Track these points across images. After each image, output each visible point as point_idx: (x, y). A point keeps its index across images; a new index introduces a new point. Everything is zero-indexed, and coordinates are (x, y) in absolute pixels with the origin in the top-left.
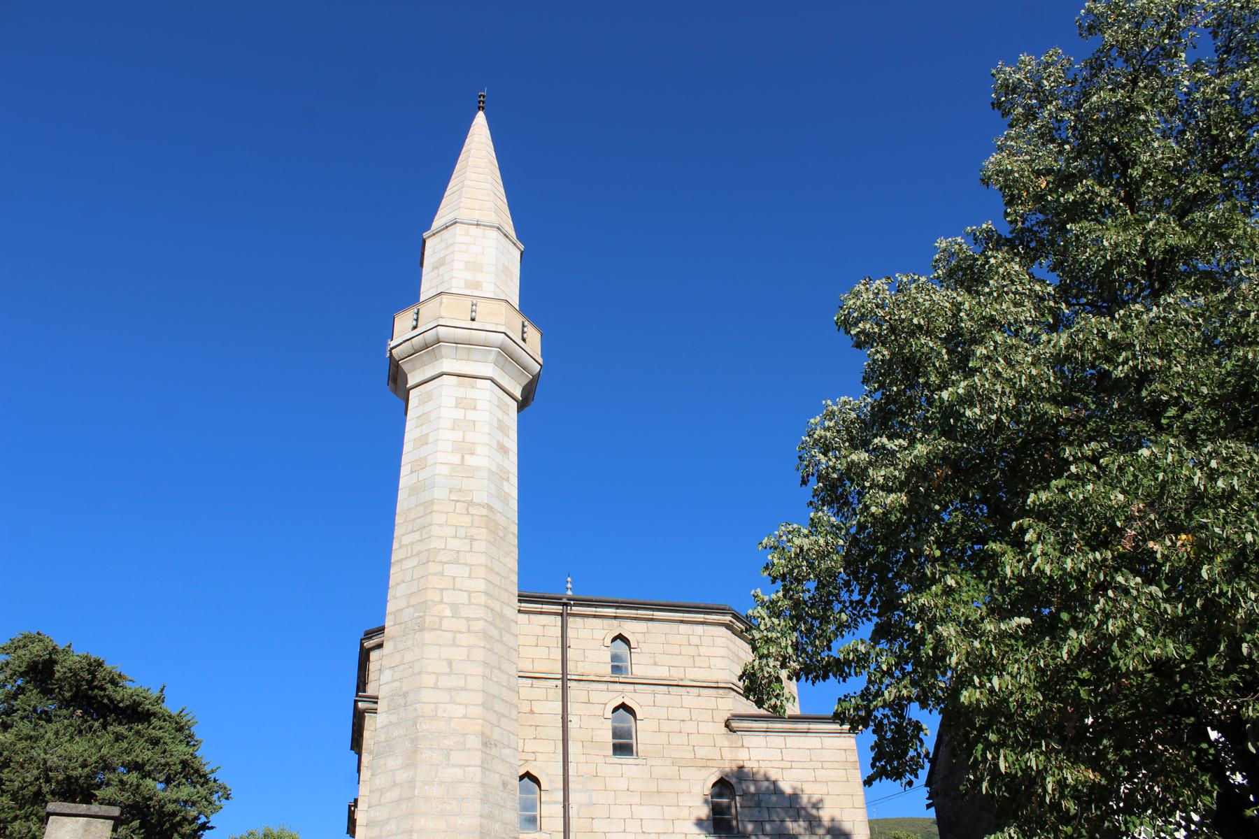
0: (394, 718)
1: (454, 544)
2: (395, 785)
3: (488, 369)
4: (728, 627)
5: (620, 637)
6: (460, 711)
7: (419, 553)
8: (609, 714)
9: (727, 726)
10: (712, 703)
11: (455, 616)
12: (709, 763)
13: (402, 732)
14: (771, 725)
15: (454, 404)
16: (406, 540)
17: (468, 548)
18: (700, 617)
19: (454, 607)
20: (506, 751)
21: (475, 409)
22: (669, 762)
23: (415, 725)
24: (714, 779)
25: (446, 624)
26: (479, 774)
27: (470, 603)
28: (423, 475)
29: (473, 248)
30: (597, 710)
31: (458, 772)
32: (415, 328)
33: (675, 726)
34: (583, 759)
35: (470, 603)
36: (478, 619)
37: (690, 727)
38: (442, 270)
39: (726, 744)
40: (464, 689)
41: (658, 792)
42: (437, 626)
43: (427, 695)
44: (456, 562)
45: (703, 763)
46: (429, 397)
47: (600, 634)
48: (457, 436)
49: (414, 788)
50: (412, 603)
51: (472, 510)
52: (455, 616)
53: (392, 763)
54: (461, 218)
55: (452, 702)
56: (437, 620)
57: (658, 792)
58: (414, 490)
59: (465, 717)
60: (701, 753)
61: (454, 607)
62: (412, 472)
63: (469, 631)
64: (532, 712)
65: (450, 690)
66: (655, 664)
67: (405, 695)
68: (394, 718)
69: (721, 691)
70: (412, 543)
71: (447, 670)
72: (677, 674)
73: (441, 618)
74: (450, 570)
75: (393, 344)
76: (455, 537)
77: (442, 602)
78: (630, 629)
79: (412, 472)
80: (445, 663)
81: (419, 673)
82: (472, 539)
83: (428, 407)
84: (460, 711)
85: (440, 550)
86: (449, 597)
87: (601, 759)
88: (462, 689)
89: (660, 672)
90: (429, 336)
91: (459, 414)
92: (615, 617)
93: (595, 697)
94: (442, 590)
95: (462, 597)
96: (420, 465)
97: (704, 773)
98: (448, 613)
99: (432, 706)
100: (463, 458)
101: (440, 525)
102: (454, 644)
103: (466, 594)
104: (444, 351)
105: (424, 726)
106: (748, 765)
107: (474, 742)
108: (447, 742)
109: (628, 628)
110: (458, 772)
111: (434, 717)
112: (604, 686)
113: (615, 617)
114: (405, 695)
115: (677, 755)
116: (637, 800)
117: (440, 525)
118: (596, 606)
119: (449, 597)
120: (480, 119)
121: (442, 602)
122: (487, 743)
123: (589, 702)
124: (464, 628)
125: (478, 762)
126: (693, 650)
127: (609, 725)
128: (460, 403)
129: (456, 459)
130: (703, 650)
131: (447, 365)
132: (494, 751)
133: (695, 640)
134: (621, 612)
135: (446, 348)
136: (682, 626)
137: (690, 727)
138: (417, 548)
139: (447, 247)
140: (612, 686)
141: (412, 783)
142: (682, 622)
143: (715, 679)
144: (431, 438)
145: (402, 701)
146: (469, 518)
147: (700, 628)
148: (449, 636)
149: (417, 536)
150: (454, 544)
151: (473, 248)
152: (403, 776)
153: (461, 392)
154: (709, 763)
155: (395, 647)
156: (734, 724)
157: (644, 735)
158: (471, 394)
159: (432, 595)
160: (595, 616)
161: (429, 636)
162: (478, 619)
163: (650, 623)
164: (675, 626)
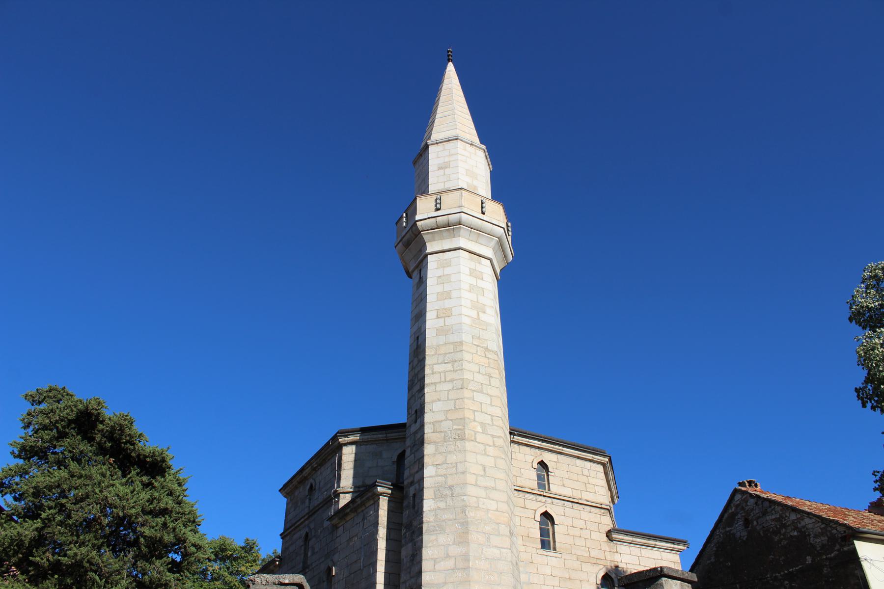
0: (442, 505)
1: (480, 378)
2: (448, 556)
3: (489, 253)
4: (604, 465)
5: (542, 464)
7: (452, 381)
9: (607, 536)
10: (598, 518)
12: (599, 562)
14: (634, 539)
16: (437, 368)
18: (590, 456)
19: (483, 424)
22: (575, 558)
23: (464, 512)
24: (602, 574)
25: (480, 437)
27: (493, 425)
28: (449, 321)
29: (459, 161)
31: (497, 551)
33: (577, 532)
34: (522, 548)
36: (499, 437)
37: (586, 534)
38: (447, 171)
39: (607, 549)
40: (494, 489)
41: (570, 579)
43: (471, 490)
44: (481, 392)
45: (594, 561)
46: (448, 264)
47: (529, 459)
49: (469, 560)
51: (489, 355)
53: (442, 539)
54: (461, 135)
55: (488, 498)
57: (570, 579)
58: (440, 331)
60: (594, 553)
61: (483, 424)
62: (438, 317)
63: (494, 445)
65: (486, 488)
66: (564, 485)
67: (451, 488)
68: (442, 505)
69: (603, 511)
71: (482, 473)
72: (577, 495)
73: (476, 433)
74: (479, 397)
75: (417, 218)
76: (479, 372)
77: (475, 420)
78: (548, 458)
79: (438, 317)
80: (481, 467)
81: (464, 473)
82: (490, 377)
83: (448, 271)
84: (493, 505)
86: (480, 417)
87: (534, 551)
88: (493, 488)
89: (566, 492)
90: (453, 218)
91: (473, 281)
92: (539, 448)
93: (529, 504)
94: (474, 411)
95: (487, 419)
96: (445, 314)
97: (596, 569)
98: (479, 429)
103: (489, 417)
104: (462, 231)
105: (471, 514)
106: (621, 565)
107: (504, 530)
108: (487, 528)
109: (548, 458)
111: (477, 508)
112: (533, 497)
113: (539, 448)
115: (579, 553)
116: (556, 583)
118: (529, 438)
119: (480, 417)
120: (451, 67)
121: (475, 420)
124: (491, 443)
126: (584, 479)
127: (537, 526)
128: (473, 273)
130: (591, 480)
131: (462, 242)
133: (586, 472)
134: (544, 445)
135: (464, 230)
136: (578, 461)
137: (586, 534)
138: (449, 377)
139: (450, 155)
140: (538, 497)
141: (466, 558)
142: (578, 458)
143: (599, 501)
144: (454, 294)
145: (448, 492)
147: (588, 464)
148: (482, 446)
149: (449, 367)
150: (480, 378)
151: (459, 161)
152: (456, 551)
153: (473, 265)
154: (599, 562)
156: (614, 536)
158: (479, 268)
159: (468, 414)
160: (526, 445)
161: (469, 445)
162: (499, 437)
163: (559, 456)
164: (574, 460)
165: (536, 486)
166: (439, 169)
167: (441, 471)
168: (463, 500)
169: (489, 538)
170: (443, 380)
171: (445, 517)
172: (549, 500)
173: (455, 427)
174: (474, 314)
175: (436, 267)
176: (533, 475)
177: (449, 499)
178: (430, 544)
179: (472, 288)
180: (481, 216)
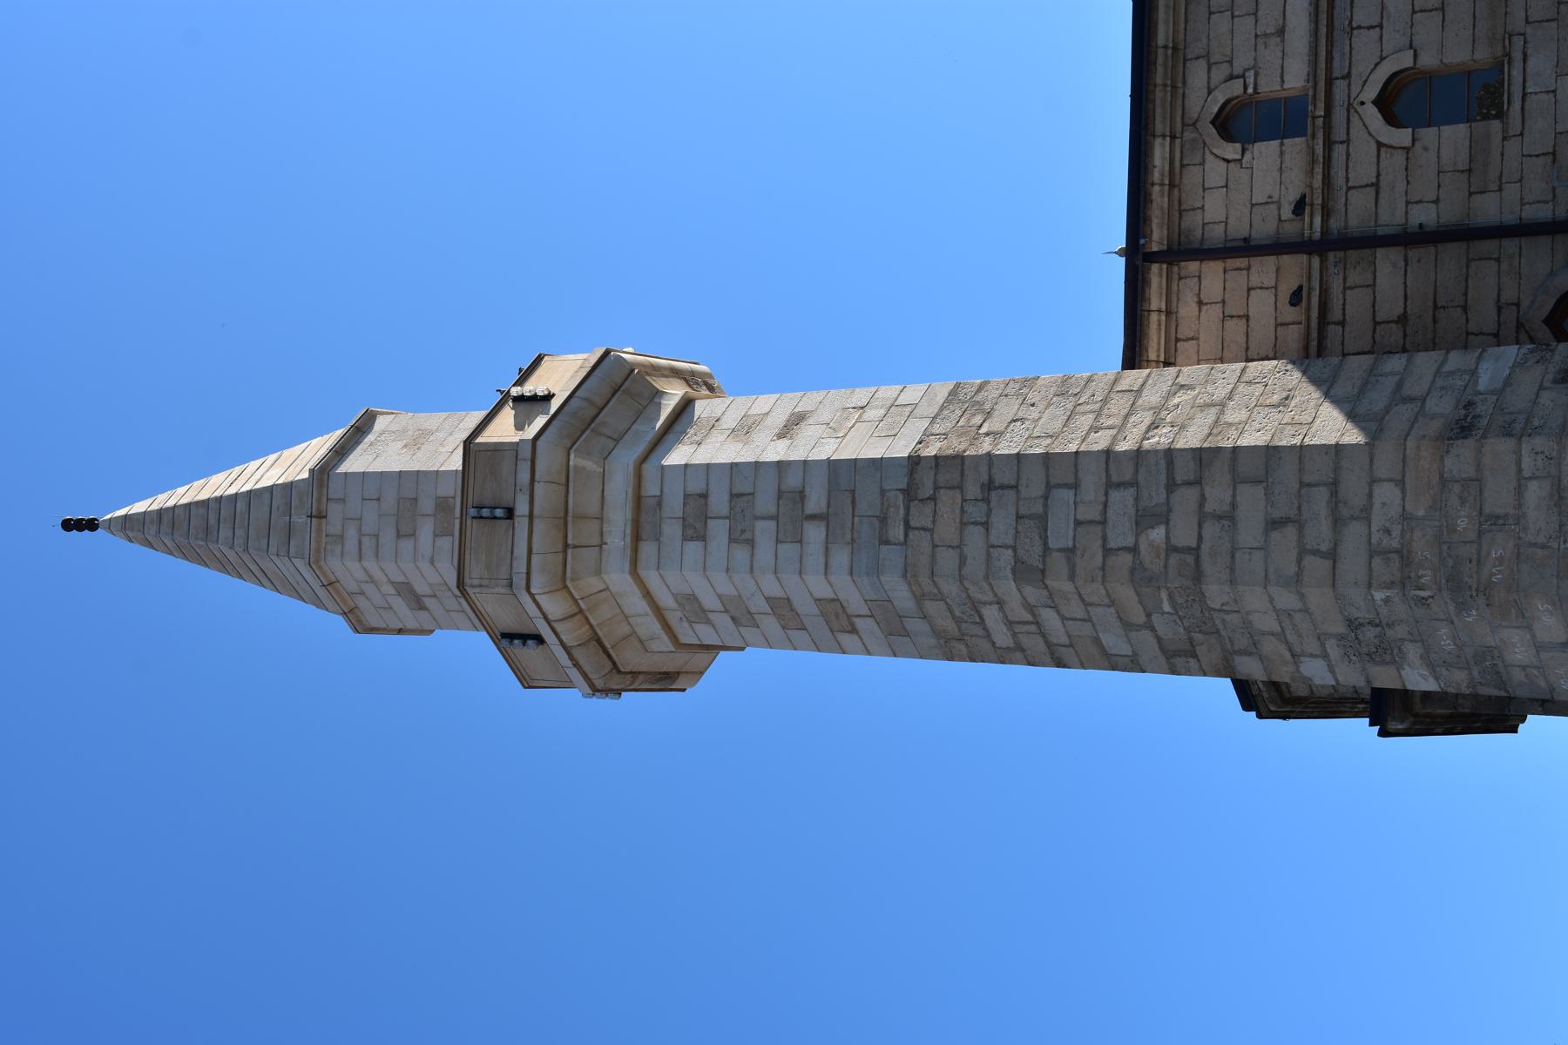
0: (1413, 652)
6: (1386, 493)
7: (1030, 608)
8: (1403, 136)
11: (1163, 517)
13: (1444, 631)
15: (700, 544)
17: (1011, 494)
19: (1144, 519)
20: (1484, 383)
21: (704, 496)
25: (1184, 535)
26: (1539, 442)
30: (1393, 164)
32: (539, 640)
34: (1512, 191)
35: (1134, 483)
38: (421, 588)
42: (1190, 559)
44: (1042, 520)
48: (764, 531)
50: (1142, 619)
51: (926, 491)
52: (1163, 517)
55: (1365, 514)
56: (1174, 559)
59: (1401, 483)
61: (1144, 519)
63: (1198, 482)
64: (1403, 319)
65: (1337, 522)
66: (1281, 32)
67: (1353, 625)
70: (1010, 624)
71: (1291, 531)
73: (1171, 549)
76: (986, 525)
77: (1134, 550)
80: (1275, 535)
84: (1386, 493)
85: (1017, 560)
86: (1121, 535)
87: (1513, 147)
88: (1334, 493)
93: (1363, 171)
94: (1107, 552)
98: (1157, 534)
99: (1377, 561)
100: (812, 517)
101: (963, 560)
102: (1229, 517)
103: (1115, 495)
107: (1461, 458)
108: (1462, 524)
110: (1535, 492)
112: (1339, 151)
114: (1353, 625)
117: (963, 560)
122: (1463, 428)
123: (1376, 186)
124: (1191, 494)
125: (1510, 443)
129: (815, 534)
132: (1484, 408)
140: (1339, 134)
145: (1370, 633)
146: (944, 496)
148: (1210, 529)
149: (991, 614)
153: (672, 530)
155: (1244, 652)
157: (1451, 47)
165: (1296, 145)
166: (423, 608)
167: (1312, 646)
168: (1387, 601)
169: (1497, 520)
170: (1033, 628)
171: (1448, 644)
172: (1340, 88)
173: (1167, 607)
174: (815, 534)
175: (709, 629)
176: (1265, 151)
177: (1390, 633)
178: (1543, 684)
179: (742, 537)
180: (521, 524)
